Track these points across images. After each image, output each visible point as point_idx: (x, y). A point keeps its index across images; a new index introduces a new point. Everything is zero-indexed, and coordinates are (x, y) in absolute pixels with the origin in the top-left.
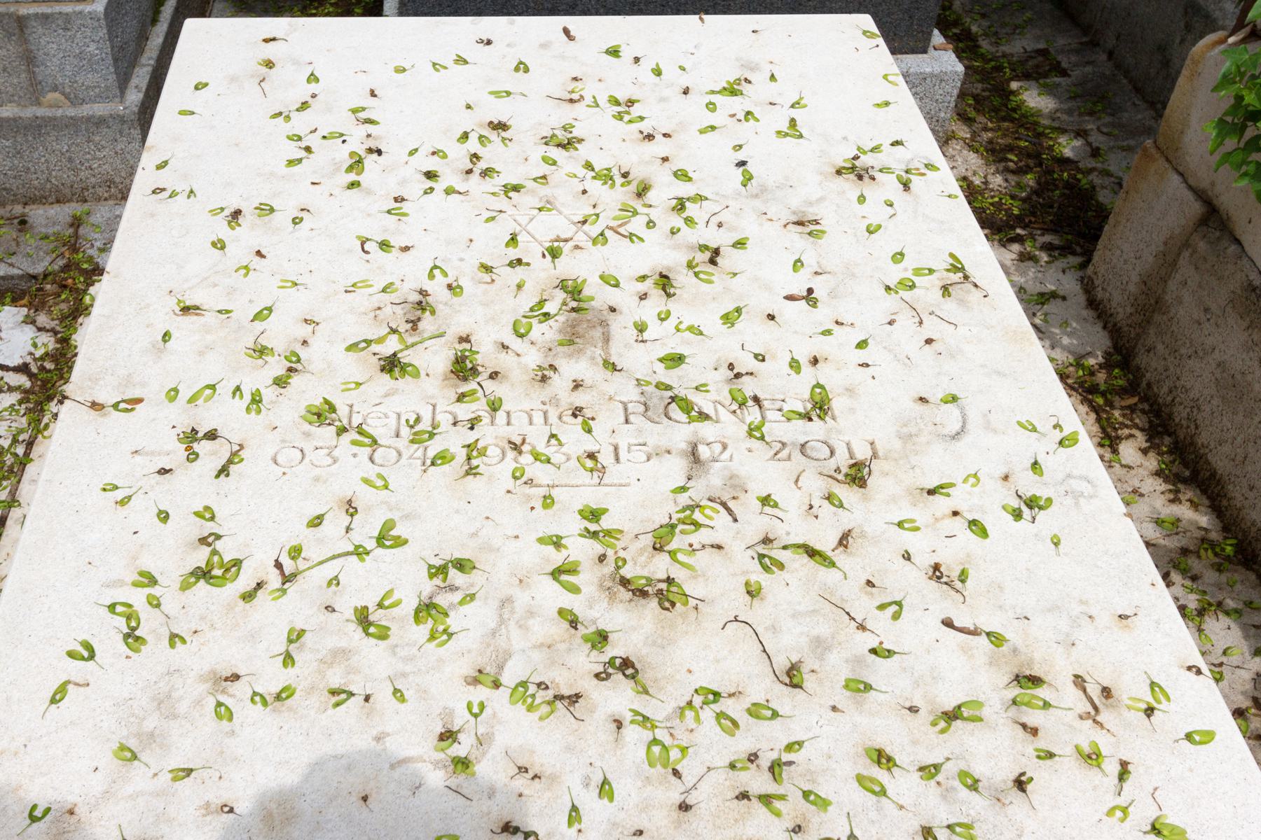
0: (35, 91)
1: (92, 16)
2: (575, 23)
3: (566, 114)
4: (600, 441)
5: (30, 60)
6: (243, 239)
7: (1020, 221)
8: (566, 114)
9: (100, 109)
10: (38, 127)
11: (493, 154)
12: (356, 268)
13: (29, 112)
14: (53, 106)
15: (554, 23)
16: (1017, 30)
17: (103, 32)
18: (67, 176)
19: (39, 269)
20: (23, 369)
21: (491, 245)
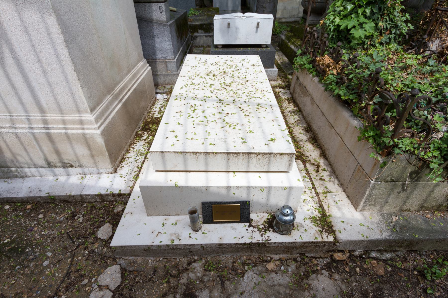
0: (167, 70)
1: (174, 61)
2: (227, 55)
3: (226, 61)
4: (226, 79)
5: (167, 67)
6: (194, 68)
7: (285, 87)
8: (226, 61)
9: (175, 73)
10: (167, 75)
11: (218, 63)
12: (205, 70)
13: (166, 73)
14: (169, 72)
15: (226, 55)
16: (290, 70)
17: (176, 63)
18: (170, 82)
19: (167, 91)
20: (166, 99)
21: (218, 69)
